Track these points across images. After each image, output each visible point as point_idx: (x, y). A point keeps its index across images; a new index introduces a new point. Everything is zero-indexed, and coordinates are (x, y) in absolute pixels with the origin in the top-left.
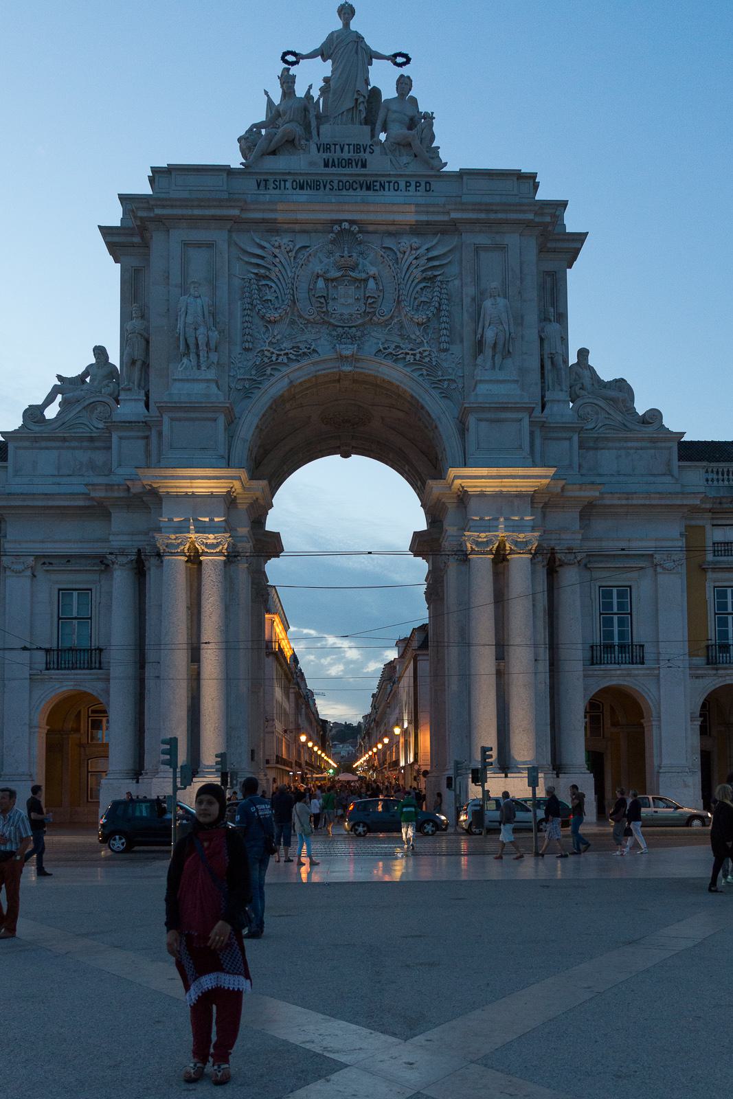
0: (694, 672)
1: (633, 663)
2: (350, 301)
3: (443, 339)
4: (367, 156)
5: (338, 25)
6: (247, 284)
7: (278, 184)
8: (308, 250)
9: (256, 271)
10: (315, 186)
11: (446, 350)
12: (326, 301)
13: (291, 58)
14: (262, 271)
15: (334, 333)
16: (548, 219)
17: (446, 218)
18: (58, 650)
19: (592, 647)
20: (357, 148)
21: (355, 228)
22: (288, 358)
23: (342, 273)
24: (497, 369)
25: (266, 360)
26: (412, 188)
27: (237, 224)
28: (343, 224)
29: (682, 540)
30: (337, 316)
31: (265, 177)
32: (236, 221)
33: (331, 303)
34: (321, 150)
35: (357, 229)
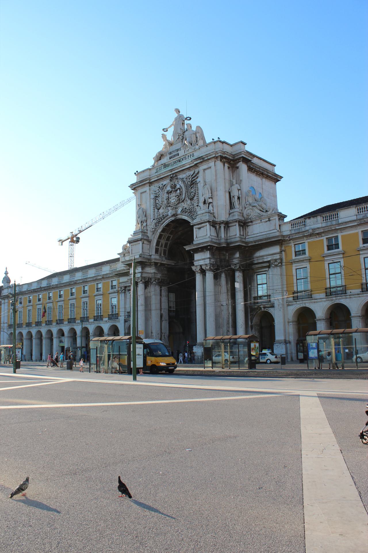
2: (174, 198)
5: (176, 115)
11: (198, 206)
12: (168, 199)
13: (165, 130)
20: (177, 150)
22: (162, 220)
31: (157, 168)
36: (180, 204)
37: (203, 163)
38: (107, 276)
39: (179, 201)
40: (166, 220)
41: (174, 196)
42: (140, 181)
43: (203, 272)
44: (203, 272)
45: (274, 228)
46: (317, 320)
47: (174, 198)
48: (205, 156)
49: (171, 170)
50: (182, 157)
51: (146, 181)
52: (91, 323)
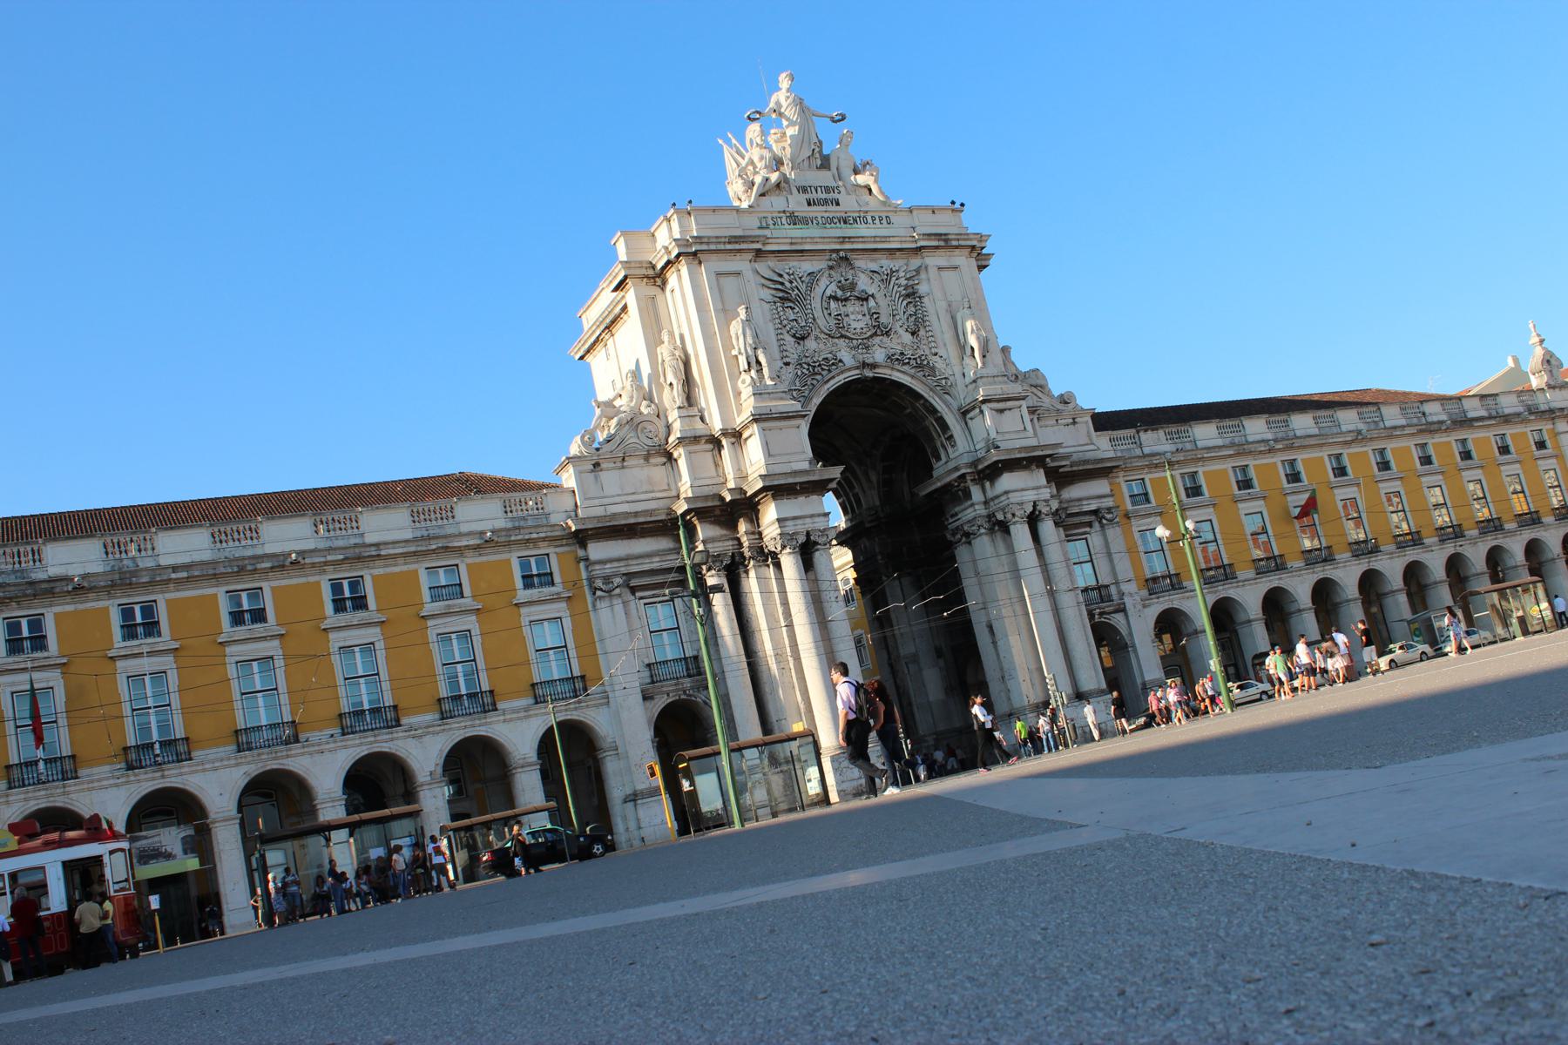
1: (1102, 602)
3: (933, 344)
4: (836, 196)
9: (781, 294)
10: (805, 221)
11: (936, 354)
17: (914, 246)
20: (828, 190)
23: (849, 294)
26: (877, 221)
27: (759, 254)
31: (765, 215)
32: (759, 254)
33: (846, 319)
36: (877, 340)
37: (939, 252)
38: (513, 538)
40: (838, 375)
41: (858, 313)
42: (735, 237)
43: (1033, 520)
44: (1033, 520)
45: (1087, 441)
47: (860, 317)
48: (953, 237)
49: (844, 238)
51: (753, 242)
52: (416, 733)
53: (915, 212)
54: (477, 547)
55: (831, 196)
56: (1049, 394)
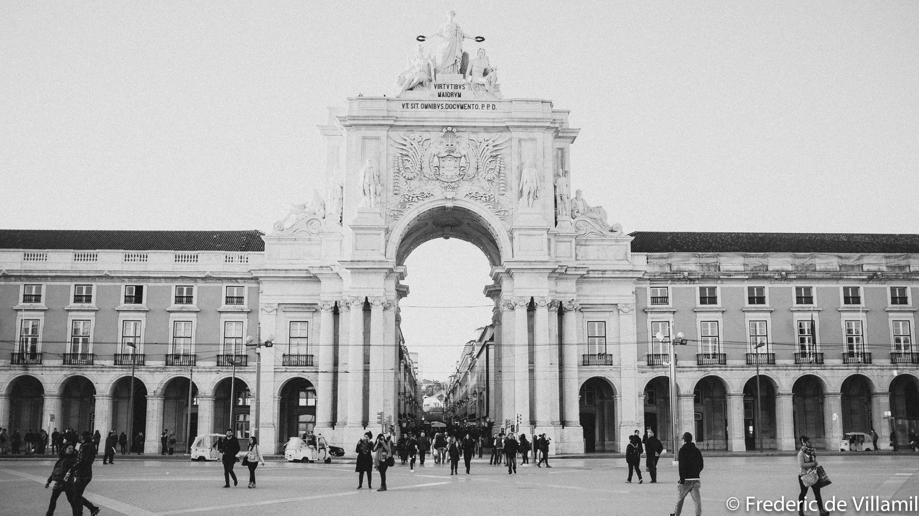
0: (640, 369)
1: (606, 365)
2: (451, 169)
3: (501, 189)
6: (397, 159)
7: (413, 105)
8: (430, 141)
10: (434, 106)
11: (503, 195)
14: (405, 153)
15: (443, 185)
16: (557, 125)
17: (504, 125)
18: (289, 355)
19: (584, 355)
20: (456, 87)
21: (454, 130)
22: (418, 199)
24: (530, 206)
25: (406, 200)
28: (449, 127)
29: (633, 296)
30: (445, 176)
31: (407, 102)
32: (391, 126)
34: (437, 87)
35: (456, 130)
38: (222, 276)
39: (463, 178)
43: (532, 307)
44: (532, 307)
46: (684, 396)
47: (452, 168)
50: (469, 103)
53: (513, 102)
54: (203, 279)
55: (459, 90)
56: (604, 225)
